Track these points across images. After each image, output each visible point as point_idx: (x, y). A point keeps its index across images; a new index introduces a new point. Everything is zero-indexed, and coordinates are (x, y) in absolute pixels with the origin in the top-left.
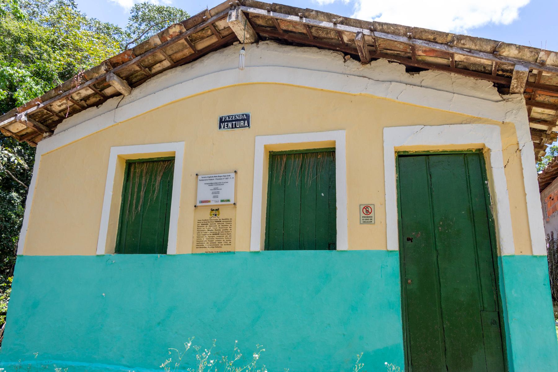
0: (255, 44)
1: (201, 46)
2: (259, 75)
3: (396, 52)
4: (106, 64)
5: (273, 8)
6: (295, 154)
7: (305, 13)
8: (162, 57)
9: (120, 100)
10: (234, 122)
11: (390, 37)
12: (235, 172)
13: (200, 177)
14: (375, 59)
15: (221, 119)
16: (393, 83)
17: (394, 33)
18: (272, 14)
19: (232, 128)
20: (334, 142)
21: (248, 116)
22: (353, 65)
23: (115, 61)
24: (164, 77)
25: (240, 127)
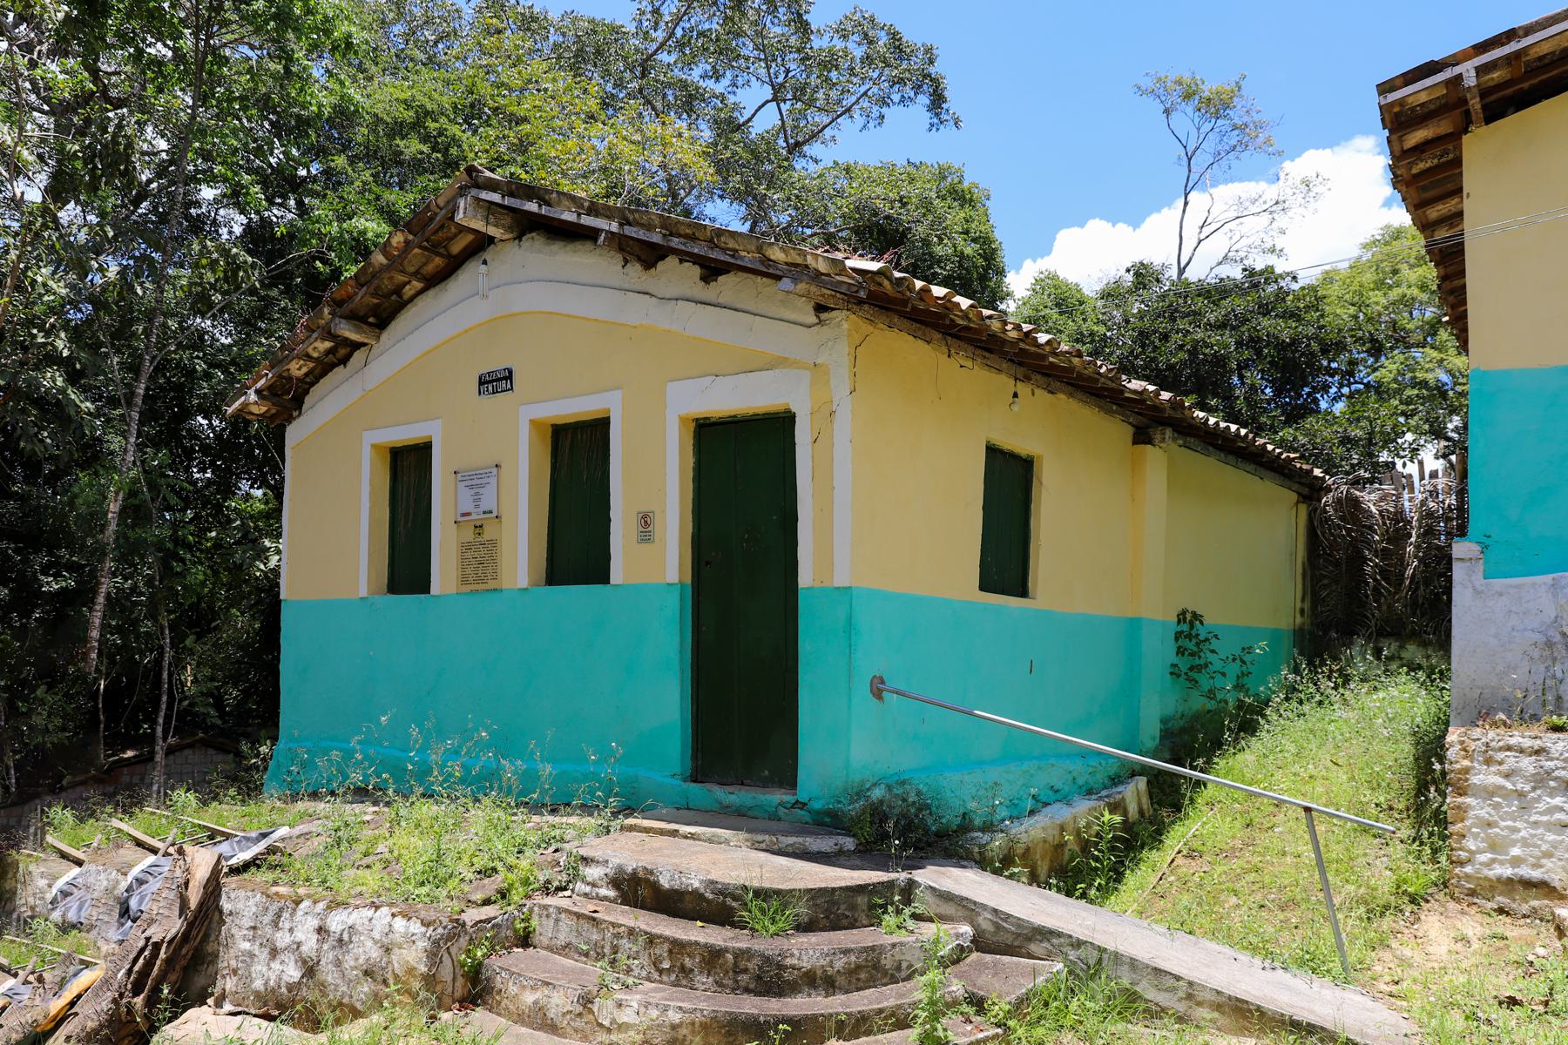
8: (401, 278)
10: (496, 382)
21: (510, 372)
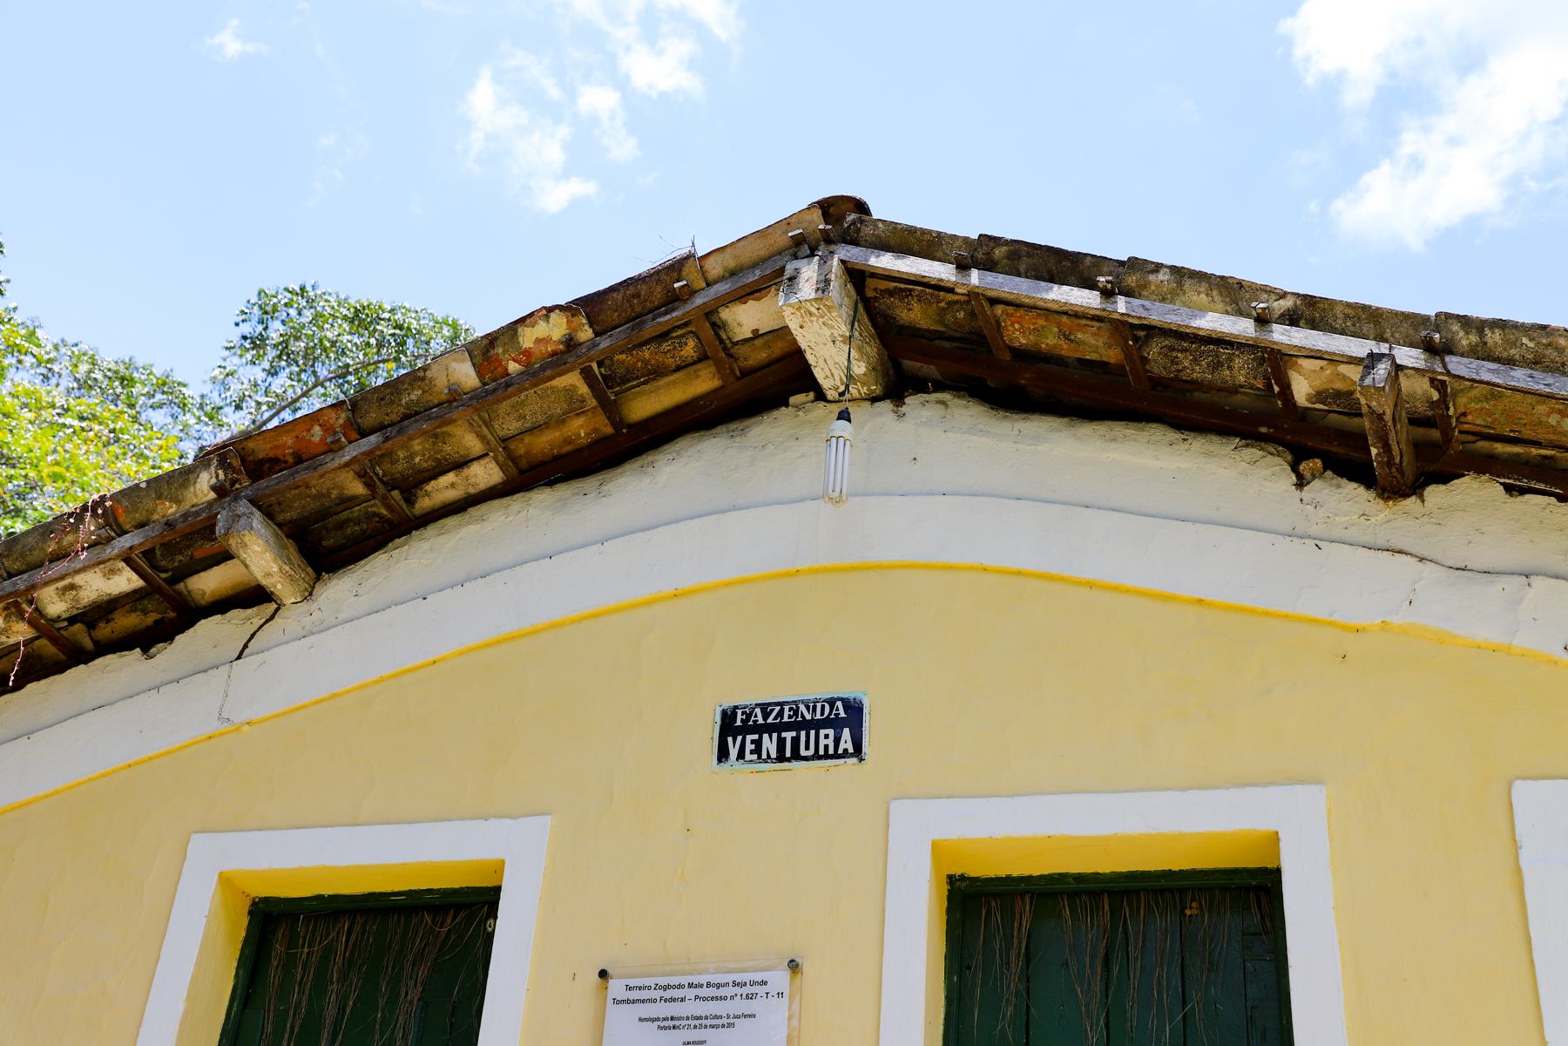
0: (886, 406)
1: (645, 405)
2: (904, 529)
3: (1534, 451)
4: (223, 463)
5: (984, 253)
6: (1073, 895)
7: (1127, 275)
8: (471, 443)
9: (258, 622)
11: (1520, 377)
12: (794, 966)
13: (616, 987)
14: (1445, 478)
15: (728, 717)
16: (1537, 582)
17: (1536, 363)
18: (975, 277)
19: (781, 758)
20: (1274, 839)
21: (855, 710)
22: (1342, 501)
23: (262, 449)
24: (473, 528)
25: (816, 757)
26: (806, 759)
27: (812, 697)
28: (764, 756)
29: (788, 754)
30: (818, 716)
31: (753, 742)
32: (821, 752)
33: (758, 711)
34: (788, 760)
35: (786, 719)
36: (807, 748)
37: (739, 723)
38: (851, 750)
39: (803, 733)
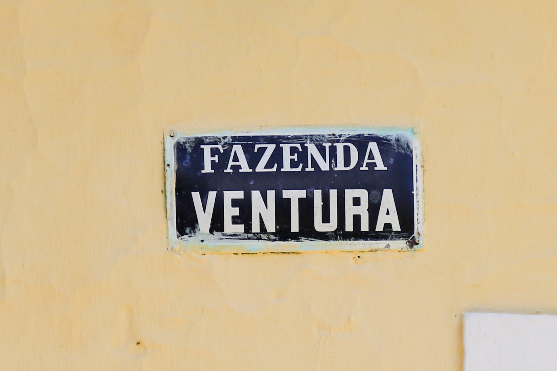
15: (188, 154)
19: (283, 233)
25: (340, 234)
26: (324, 236)
27: (326, 132)
28: (256, 228)
29: (295, 227)
30: (341, 167)
31: (235, 203)
32: (349, 227)
33: (238, 149)
34: (295, 237)
35: (287, 167)
36: (326, 219)
37: (208, 169)
38: (396, 227)
39: (318, 194)
